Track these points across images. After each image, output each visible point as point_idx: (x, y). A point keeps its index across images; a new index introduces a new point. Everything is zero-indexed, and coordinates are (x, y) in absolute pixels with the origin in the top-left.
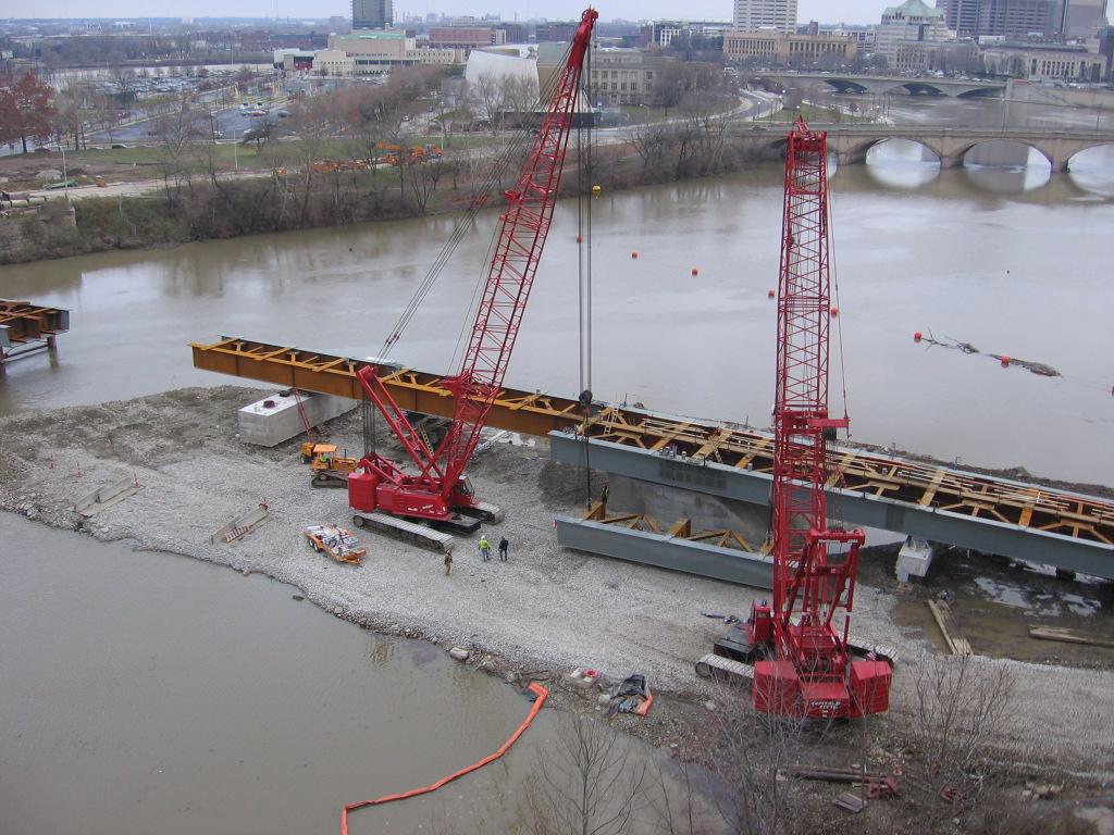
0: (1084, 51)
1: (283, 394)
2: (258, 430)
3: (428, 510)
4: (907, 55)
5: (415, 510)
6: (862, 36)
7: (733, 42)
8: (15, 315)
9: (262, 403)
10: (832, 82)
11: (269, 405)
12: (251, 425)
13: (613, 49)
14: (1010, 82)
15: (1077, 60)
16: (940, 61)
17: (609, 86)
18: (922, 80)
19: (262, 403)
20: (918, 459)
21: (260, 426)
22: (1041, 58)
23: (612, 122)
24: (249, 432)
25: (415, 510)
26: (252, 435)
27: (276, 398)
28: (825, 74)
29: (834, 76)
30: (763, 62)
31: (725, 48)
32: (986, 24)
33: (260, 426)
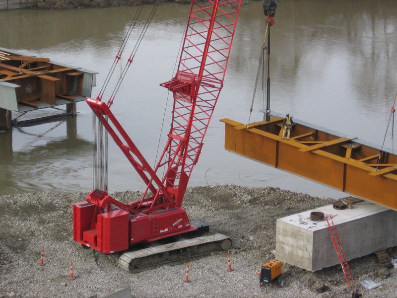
1: (340, 206)
2: (298, 247)
3: (176, 226)
5: (166, 230)
8: (29, 73)
9: (307, 214)
11: (318, 217)
12: (291, 240)
19: (307, 214)
20: (121, 53)
21: (301, 243)
24: (287, 249)
25: (166, 230)
26: (291, 254)
27: (327, 210)
33: (301, 243)
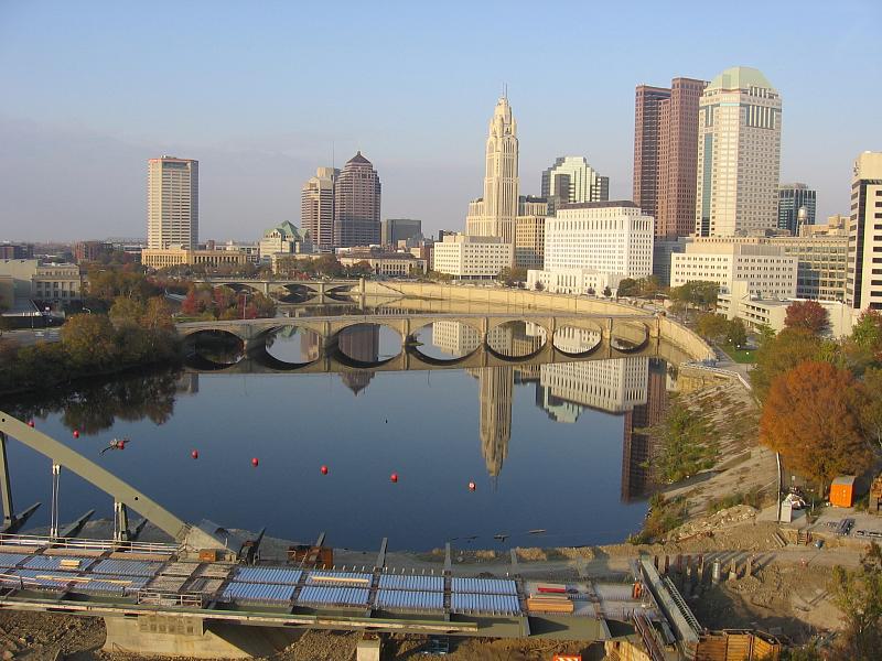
0: (412, 257)
4: (286, 262)
6: (249, 252)
7: (149, 258)
10: (230, 285)
13: (53, 264)
14: (361, 280)
15: (408, 262)
16: (310, 269)
17: (52, 294)
18: (298, 282)
22: (379, 262)
23: (58, 322)
28: (224, 280)
29: (231, 280)
30: (174, 269)
31: (144, 263)
32: (337, 238)
